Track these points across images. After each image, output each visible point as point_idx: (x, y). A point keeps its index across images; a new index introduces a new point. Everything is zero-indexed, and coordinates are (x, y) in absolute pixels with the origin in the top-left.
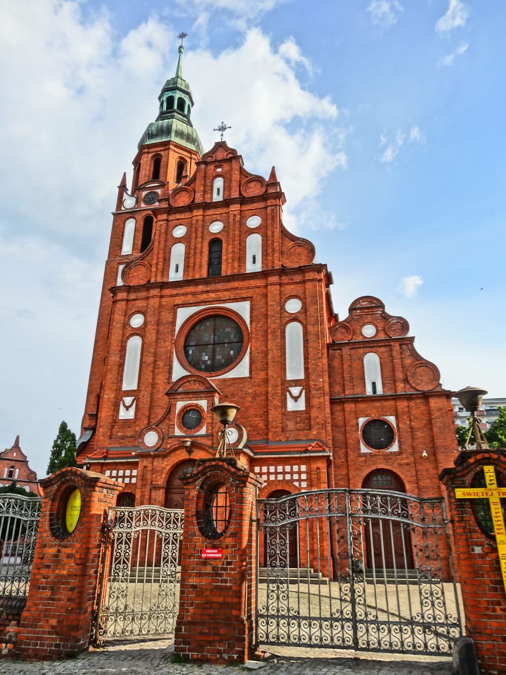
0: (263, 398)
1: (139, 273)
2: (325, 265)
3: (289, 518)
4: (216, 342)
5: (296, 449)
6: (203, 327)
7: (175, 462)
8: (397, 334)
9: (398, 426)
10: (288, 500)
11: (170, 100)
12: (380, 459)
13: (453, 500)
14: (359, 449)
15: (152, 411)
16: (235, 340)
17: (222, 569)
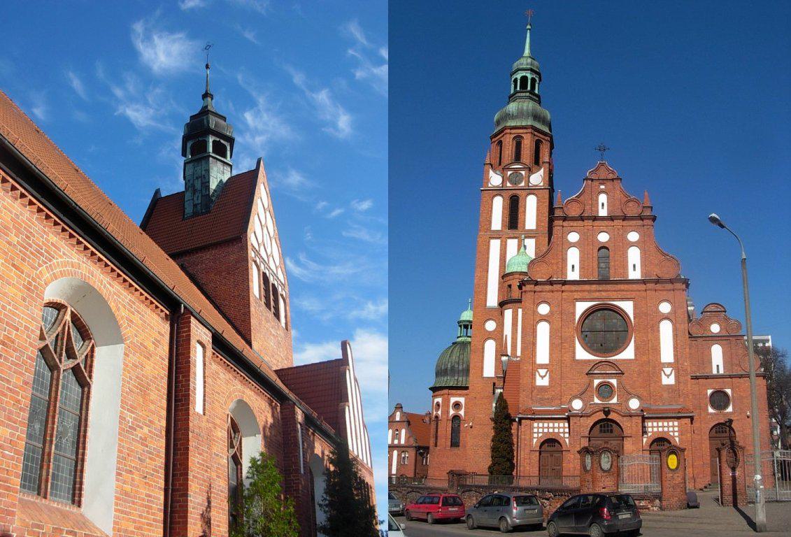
9: (733, 395)
16: (620, 329)
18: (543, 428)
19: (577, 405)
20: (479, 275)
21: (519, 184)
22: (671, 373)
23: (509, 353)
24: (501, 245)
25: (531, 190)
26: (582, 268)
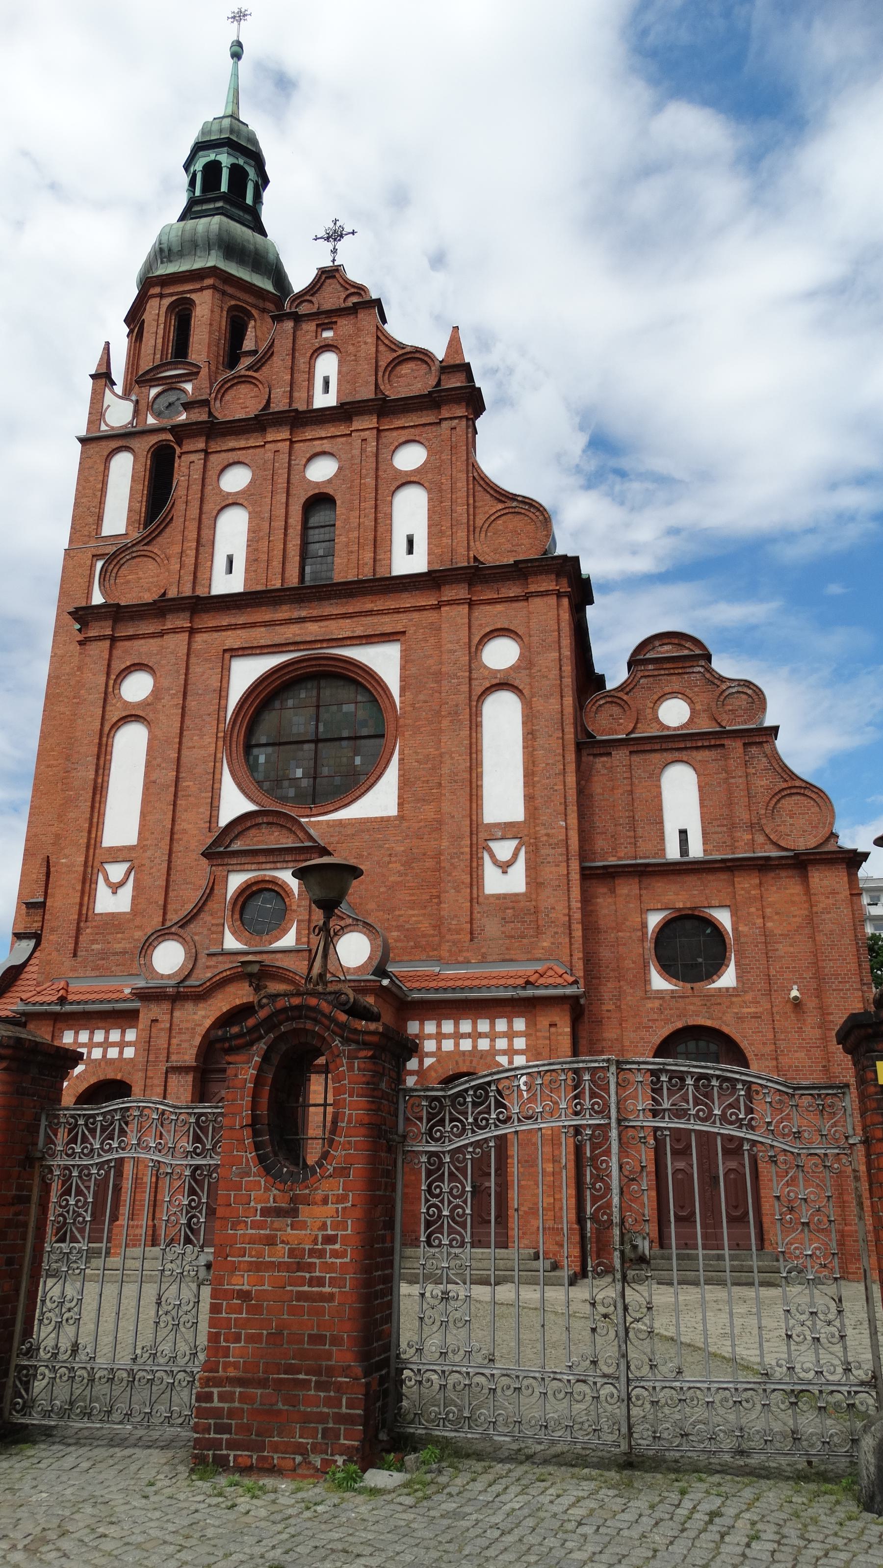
0: (430, 863)
1: (141, 574)
2: (576, 560)
3: (473, 1132)
4: (321, 736)
5: (502, 982)
6: (290, 703)
7: (225, 1010)
8: (738, 720)
9: (735, 929)
10: (472, 1087)
11: (213, 169)
12: (692, 1004)
13: (872, 1089)
14: (647, 981)
15: (171, 894)
16: (365, 732)
17: (312, 1253)
22: (515, 855)
26: (252, 561)
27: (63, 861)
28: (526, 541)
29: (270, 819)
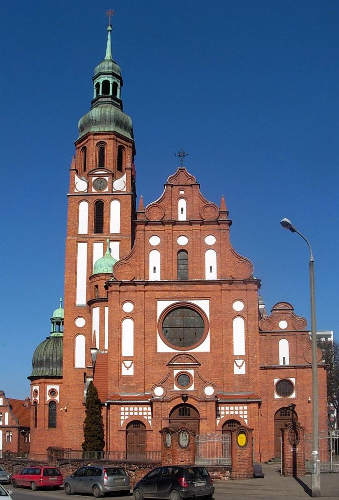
8: (300, 328)
18: (129, 411)
19: (159, 392)
20: (68, 276)
21: (104, 189)
22: (242, 364)
23: (98, 347)
24: (88, 248)
25: (115, 196)
26: (162, 270)
27: (112, 360)
28: (245, 272)
29: (185, 356)
